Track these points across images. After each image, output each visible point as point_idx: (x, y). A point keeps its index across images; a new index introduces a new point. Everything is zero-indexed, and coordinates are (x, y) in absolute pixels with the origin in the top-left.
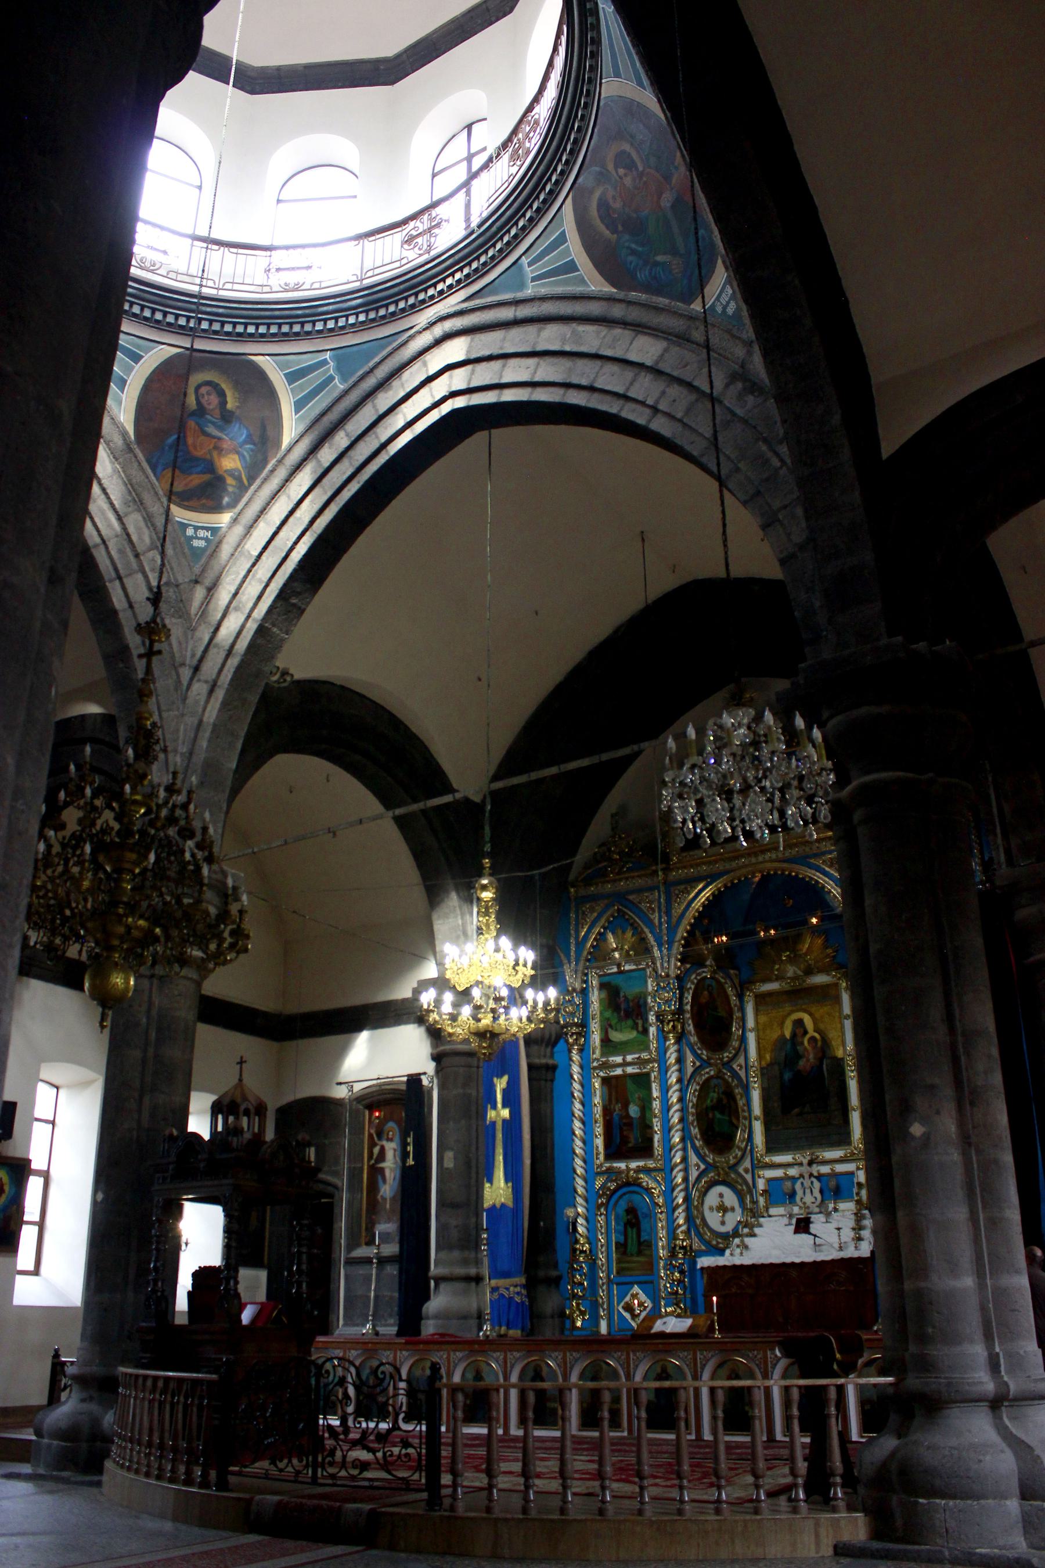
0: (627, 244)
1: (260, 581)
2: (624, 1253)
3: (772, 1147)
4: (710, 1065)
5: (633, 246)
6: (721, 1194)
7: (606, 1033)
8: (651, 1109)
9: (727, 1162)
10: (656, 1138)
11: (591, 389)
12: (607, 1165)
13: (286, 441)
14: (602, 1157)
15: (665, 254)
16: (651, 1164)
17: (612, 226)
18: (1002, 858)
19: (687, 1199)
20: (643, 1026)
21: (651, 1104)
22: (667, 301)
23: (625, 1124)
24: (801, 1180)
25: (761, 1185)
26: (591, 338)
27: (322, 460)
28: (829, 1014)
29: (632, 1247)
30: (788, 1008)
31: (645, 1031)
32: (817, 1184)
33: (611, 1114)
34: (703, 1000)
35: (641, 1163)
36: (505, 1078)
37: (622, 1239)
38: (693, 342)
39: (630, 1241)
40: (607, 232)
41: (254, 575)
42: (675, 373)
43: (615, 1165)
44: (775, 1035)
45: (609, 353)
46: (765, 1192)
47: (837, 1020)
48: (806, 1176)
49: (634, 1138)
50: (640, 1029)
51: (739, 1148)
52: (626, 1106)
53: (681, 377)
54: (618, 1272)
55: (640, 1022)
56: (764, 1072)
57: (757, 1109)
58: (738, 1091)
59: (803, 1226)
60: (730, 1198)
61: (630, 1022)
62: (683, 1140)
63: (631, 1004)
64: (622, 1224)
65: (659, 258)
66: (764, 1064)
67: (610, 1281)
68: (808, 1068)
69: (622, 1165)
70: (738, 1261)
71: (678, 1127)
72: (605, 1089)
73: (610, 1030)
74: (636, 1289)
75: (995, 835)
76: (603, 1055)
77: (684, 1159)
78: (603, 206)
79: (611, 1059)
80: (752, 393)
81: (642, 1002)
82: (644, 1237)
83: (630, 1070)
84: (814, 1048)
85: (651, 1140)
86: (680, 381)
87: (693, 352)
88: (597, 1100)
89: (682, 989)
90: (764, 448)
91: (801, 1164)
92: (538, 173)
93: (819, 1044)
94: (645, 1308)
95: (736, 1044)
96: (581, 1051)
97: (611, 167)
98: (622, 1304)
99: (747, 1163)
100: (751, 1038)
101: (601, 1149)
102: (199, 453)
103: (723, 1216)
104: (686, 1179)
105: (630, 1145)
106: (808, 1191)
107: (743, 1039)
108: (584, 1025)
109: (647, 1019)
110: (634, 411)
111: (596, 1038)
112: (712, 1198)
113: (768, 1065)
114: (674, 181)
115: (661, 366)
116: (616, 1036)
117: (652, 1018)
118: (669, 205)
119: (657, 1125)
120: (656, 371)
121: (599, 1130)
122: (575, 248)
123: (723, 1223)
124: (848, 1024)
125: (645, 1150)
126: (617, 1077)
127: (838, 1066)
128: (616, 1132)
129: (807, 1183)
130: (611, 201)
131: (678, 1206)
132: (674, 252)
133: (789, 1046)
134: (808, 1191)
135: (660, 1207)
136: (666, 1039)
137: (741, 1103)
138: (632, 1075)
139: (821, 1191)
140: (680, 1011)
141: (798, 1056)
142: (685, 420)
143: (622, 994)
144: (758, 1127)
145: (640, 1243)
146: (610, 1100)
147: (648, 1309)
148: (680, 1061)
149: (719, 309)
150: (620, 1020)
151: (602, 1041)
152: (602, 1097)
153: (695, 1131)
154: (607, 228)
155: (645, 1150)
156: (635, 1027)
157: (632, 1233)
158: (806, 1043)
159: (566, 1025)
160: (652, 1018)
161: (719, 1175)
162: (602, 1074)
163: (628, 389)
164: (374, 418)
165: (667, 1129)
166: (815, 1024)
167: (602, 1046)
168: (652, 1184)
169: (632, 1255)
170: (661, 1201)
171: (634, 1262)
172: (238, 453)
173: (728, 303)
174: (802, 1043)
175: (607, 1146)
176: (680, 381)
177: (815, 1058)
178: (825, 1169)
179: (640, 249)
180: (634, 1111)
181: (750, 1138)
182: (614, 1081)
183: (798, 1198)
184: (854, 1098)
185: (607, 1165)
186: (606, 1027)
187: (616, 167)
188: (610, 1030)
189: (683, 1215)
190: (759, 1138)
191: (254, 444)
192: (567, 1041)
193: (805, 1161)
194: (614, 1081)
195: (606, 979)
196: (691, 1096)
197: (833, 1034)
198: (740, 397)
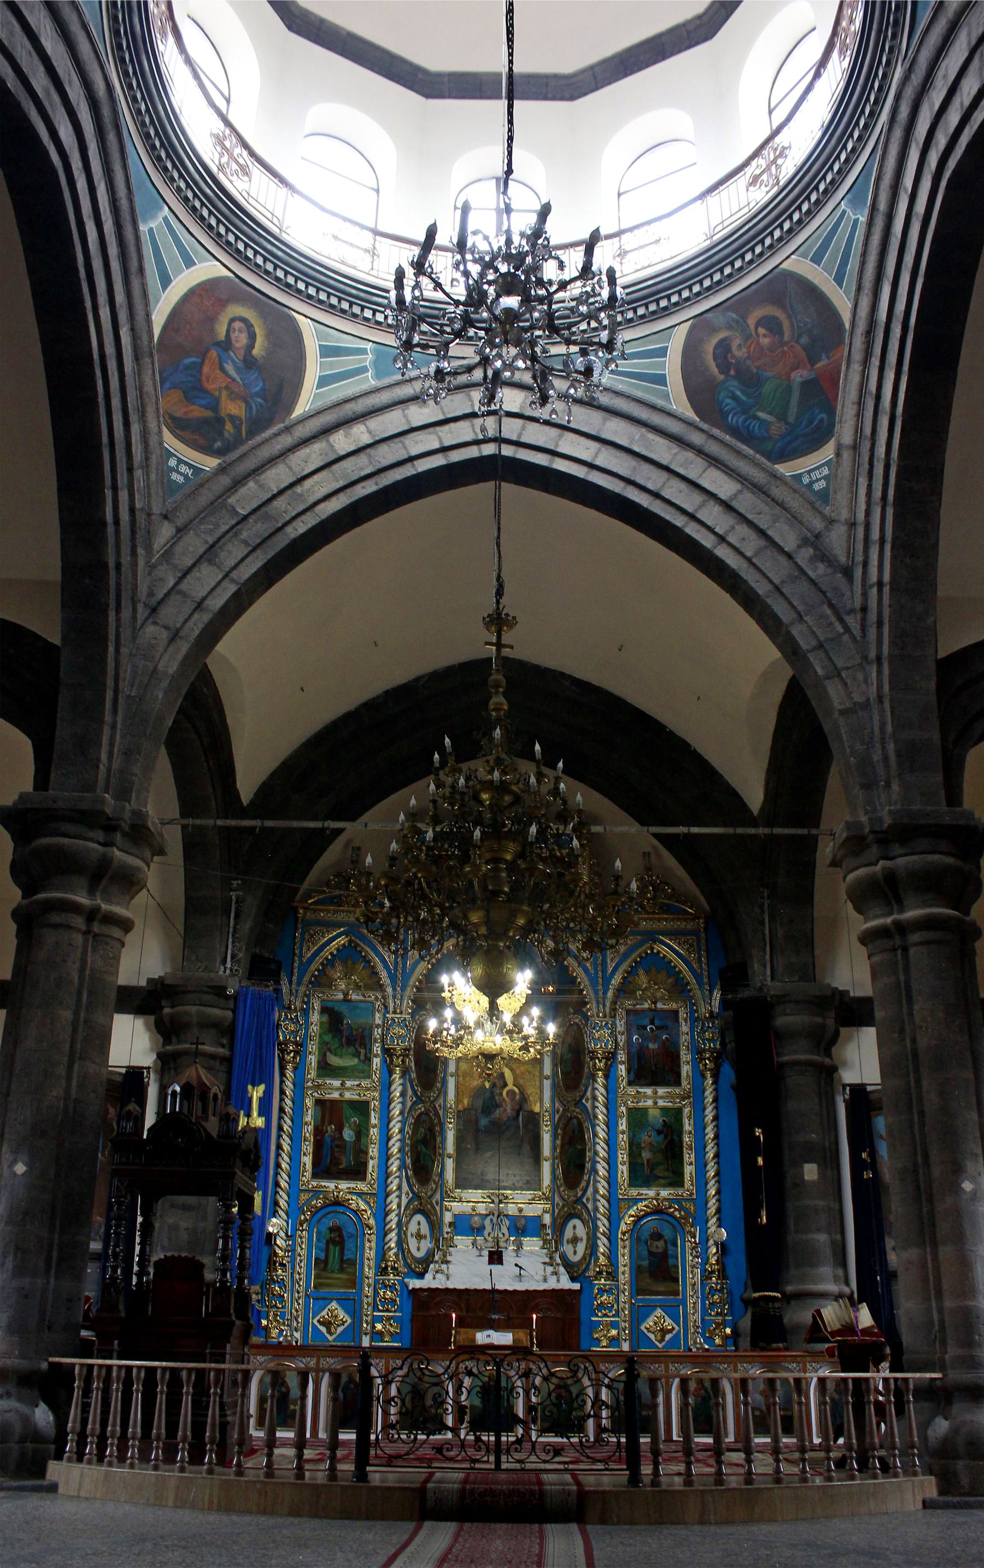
0: (732, 388)
1: (245, 543)
4: (423, 1102)
5: (738, 393)
6: (418, 1223)
7: (325, 1055)
8: (368, 1136)
9: (426, 1193)
10: (371, 1163)
11: (656, 495)
12: (315, 1184)
13: (300, 409)
14: (308, 1174)
15: (770, 413)
16: (361, 1186)
17: (724, 366)
18: (768, 972)
19: (399, 1224)
20: (366, 1055)
21: (368, 1130)
22: (751, 452)
23: (337, 1146)
24: (491, 1217)
25: (448, 1217)
26: (662, 450)
27: (337, 446)
28: (529, 1073)
29: (334, 1262)
31: (368, 1060)
33: (323, 1136)
35: (352, 1185)
36: (262, 1088)
37: (322, 1256)
38: (769, 496)
39: (331, 1260)
40: (715, 370)
41: (236, 535)
42: (750, 517)
43: (323, 1184)
45: (681, 471)
46: (451, 1224)
47: (537, 1079)
48: (496, 1214)
49: (346, 1161)
50: (362, 1057)
51: (435, 1183)
52: (340, 1129)
53: (755, 521)
54: (315, 1287)
55: (363, 1051)
56: (460, 1114)
58: (438, 1128)
59: (496, 1258)
60: (425, 1229)
61: (351, 1049)
62: (399, 1169)
65: (761, 415)
66: (460, 1108)
67: (307, 1296)
69: (330, 1185)
70: (435, 1285)
71: (398, 1156)
72: (318, 1108)
73: (328, 1054)
74: (334, 1305)
75: (765, 952)
76: (319, 1076)
77: (399, 1187)
78: (723, 348)
79: (328, 1082)
80: (822, 561)
81: (366, 1033)
82: (348, 1255)
83: (348, 1095)
84: (513, 1099)
85: (365, 1165)
86: (751, 524)
87: (767, 504)
88: (308, 1118)
90: (829, 612)
91: (493, 1202)
92: (659, 287)
93: (518, 1097)
94: (344, 1323)
95: (439, 1085)
96: (295, 1069)
97: (751, 322)
98: (318, 1318)
99: (438, 1196)
100: (451, 1083)
101: (309, 1166)
102: (210, 387)
103: (419, 1243)
104: (399, 1206)
105: (341, 1167)
106: (497, 1228)
107: (444, 1083)
110: (698, 531)
111: (313, 1059)
112: (413, 1228)
113: (465, 1109)
114: (819, 365)
115: (734, 504)
117: (377, 1048)
118: (799, 379)
119: (374, 1151)
120: (727, 506)
121: (308, 1147)
122: (672, 366)
123: (418, 1249)
124: (547, 1084)
125: (358, 1172)
126: (333, 1102)
127: (533, 1121)
128: (326, 1150)
130: (734, 348)
131: (391, 1230)
132: (782, 417)
133: (488, 1095)
134: (497, 1228)
135: (370, 1229)
136: (391, 1073)
137: (439, 1139)
138: (352, 1103)
142: (754, 560)
144: (450, 1164)
145: (342, 1261)
146: (323, 1121)
147: (346, 1325)
148: (403, 1094)
149: (806, 480)
150: (341, 1045)
151: (319, 1062)
152: (314, 1117)
153: (409, 1161)
154: (718, 366)
155: (358, 1172)
156: (357, 1054)
157: (335, 1251)
158: (504, 1093)
159: (286, 1043)
160: (377, 1048)
161: (421, 1204)
162: (316, 1094)
163: (696, 510)
164: (406, 428)
165: (386, 1156)
167: (318, 1068)
168: (363, 1206)
169: (333, 1272)
170: (372, 1222)
171: (334, 1278)
172: (246, 402)
173: (818, 480)
174: (501, 1094)
175: (315, 1164)
176: (751, 524)
177: (512, 1109)
179: (744, 398)
180: (348, 1134)
181: (441, 1175)
182: (328, 1104)
184: (546, 1149)
185: (315, 1184)
187: (758, 324)
188: (328, 1054)
189: (395, 1239)
190: (450, 1175)
191: (265, 400)
194: (328, 1104)
195: (330, 1005)
197: (531, 1091)
198: (812, 560)
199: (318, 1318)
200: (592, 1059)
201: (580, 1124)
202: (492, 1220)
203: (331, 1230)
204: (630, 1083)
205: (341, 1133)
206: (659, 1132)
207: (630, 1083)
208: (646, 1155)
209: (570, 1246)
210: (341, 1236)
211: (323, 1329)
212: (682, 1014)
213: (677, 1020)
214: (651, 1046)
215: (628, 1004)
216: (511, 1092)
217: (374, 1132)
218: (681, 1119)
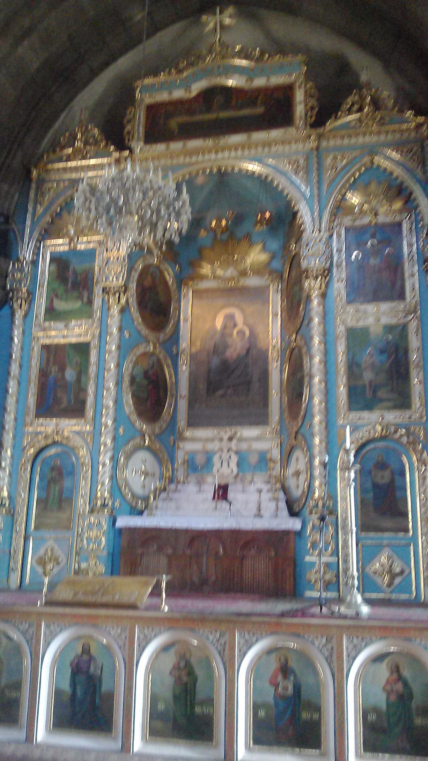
2: (45, 508)
3: (192, 423)
10: (90, 400)
19: (112, 458)
25: (180, 456)
30: (220, 302)
31: (90, 302)
32: (234, 459)
34: (148, 282)
37: (44, 495)
44: (208, 326)
48: (225, 450)
50: (85, 299)
52: (62, 369)
56: (193, 357)
57: (184, 388)
61: (75, 294)
63: (79, 278)
64: (46, 480)
66: (194, 350)
68: (235, 356)
85: (83, 403)
89: (130, 270)
108: (31, 294)
109: (91, 292)
116: (60, 305)
117: (98, 290)
121: (33, 389)
127: (263, 358)
129: (225, 456)
133: (218, 336)
134: (225, 464)
139: (238, 465)
140: (126, 288)
141: (226, 347)
143: (71, 268)
144: (183, 405)
156: (80, 297)
158: (235, 332)
166: (245, 317)
174: (231, 335)
178: (244, 446)
180: (70, 374)
183: (215, 470)
186: (52, 295)
192: (12, 307)
193: (226, 437)
196: (127, 367)
197: (259, 329)
199: (36, 557)
200: (307, 277)
201: (300, 351)
202: (221, 457)
203: (53, 469)
204: (349, 302)
205: (63, 375)
206: (382, 352)
207: (349, 302)
208: (368, 376)
209: (295, 479)
210: (61, 474)
211: (40, 570)
212: (405, 226)
213: (400, 232)
214: (373, 261)
215: (347, 221)
216: (241, 333)
217: (92, 370)
218: (407, 336)
